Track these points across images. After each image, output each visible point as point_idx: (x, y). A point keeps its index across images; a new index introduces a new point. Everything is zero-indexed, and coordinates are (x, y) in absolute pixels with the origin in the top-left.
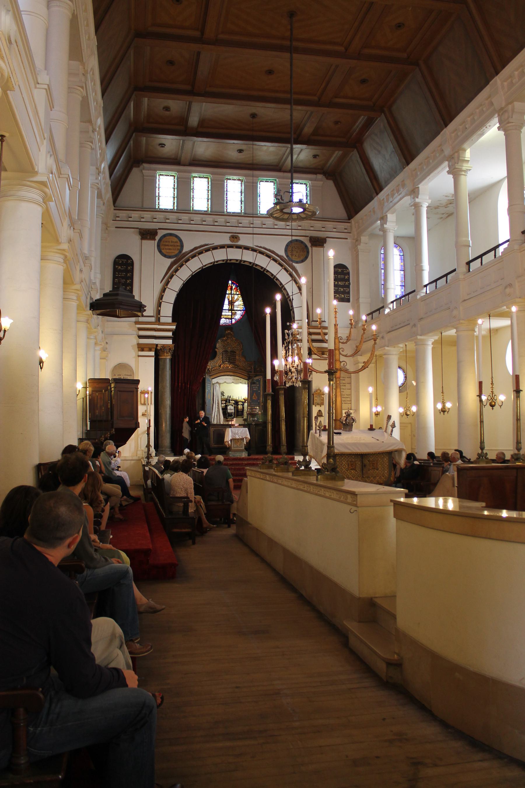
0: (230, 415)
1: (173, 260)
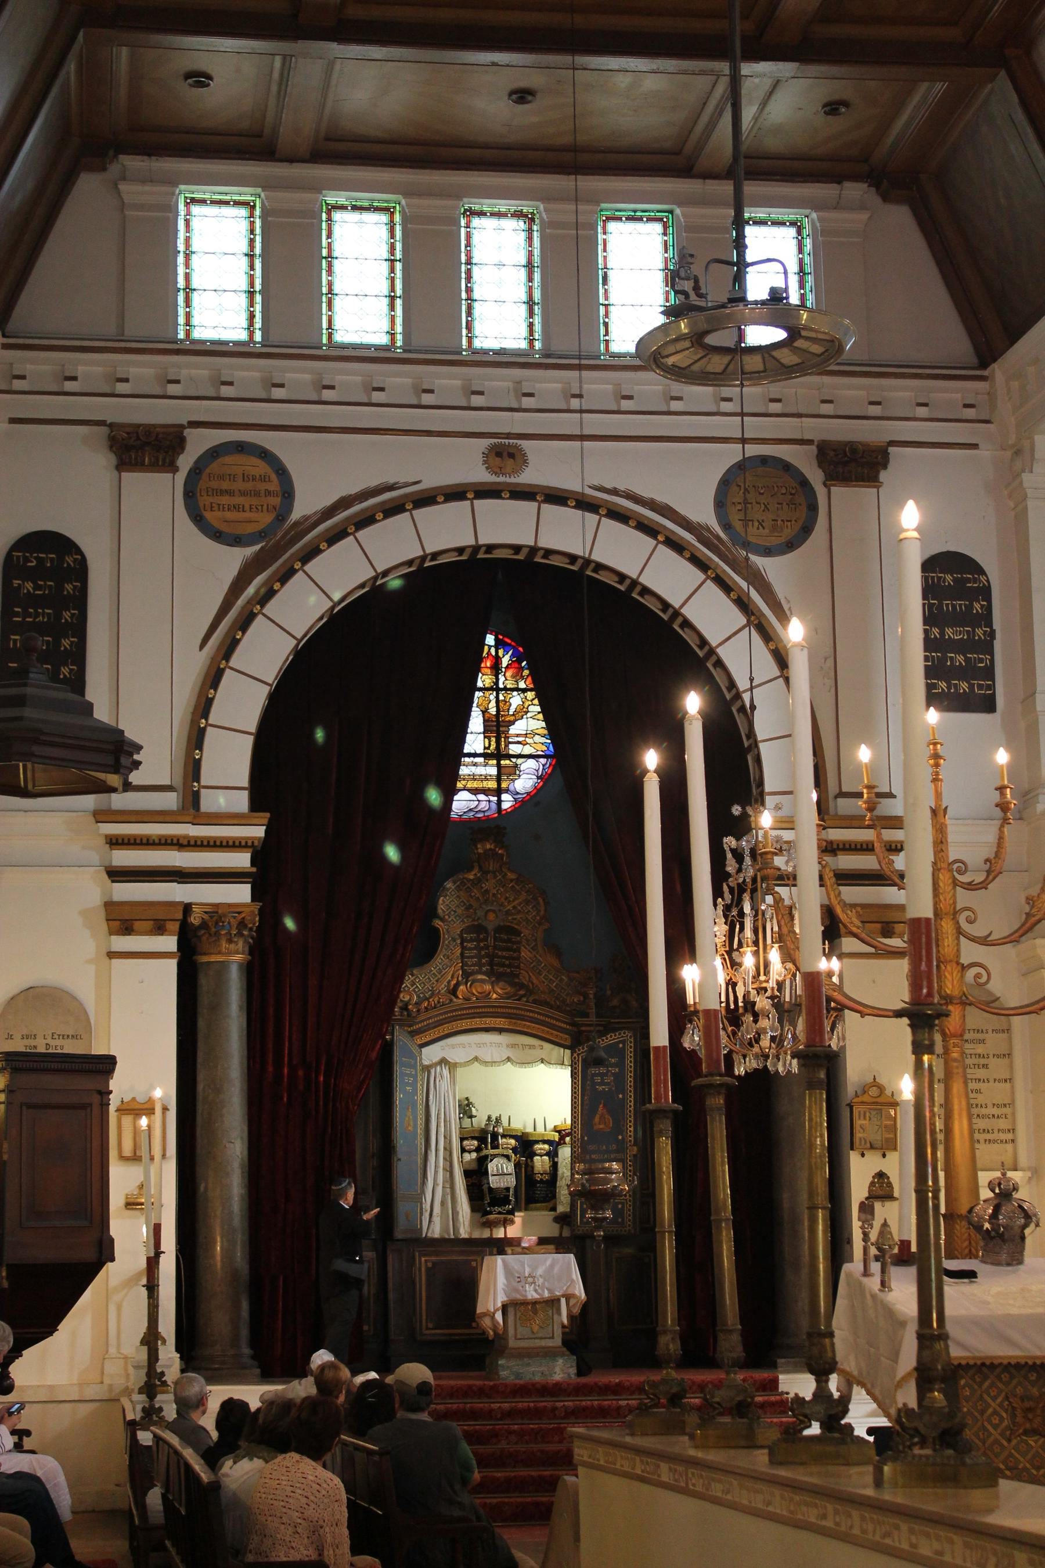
0: (499, 1198)
1: (250, 551)
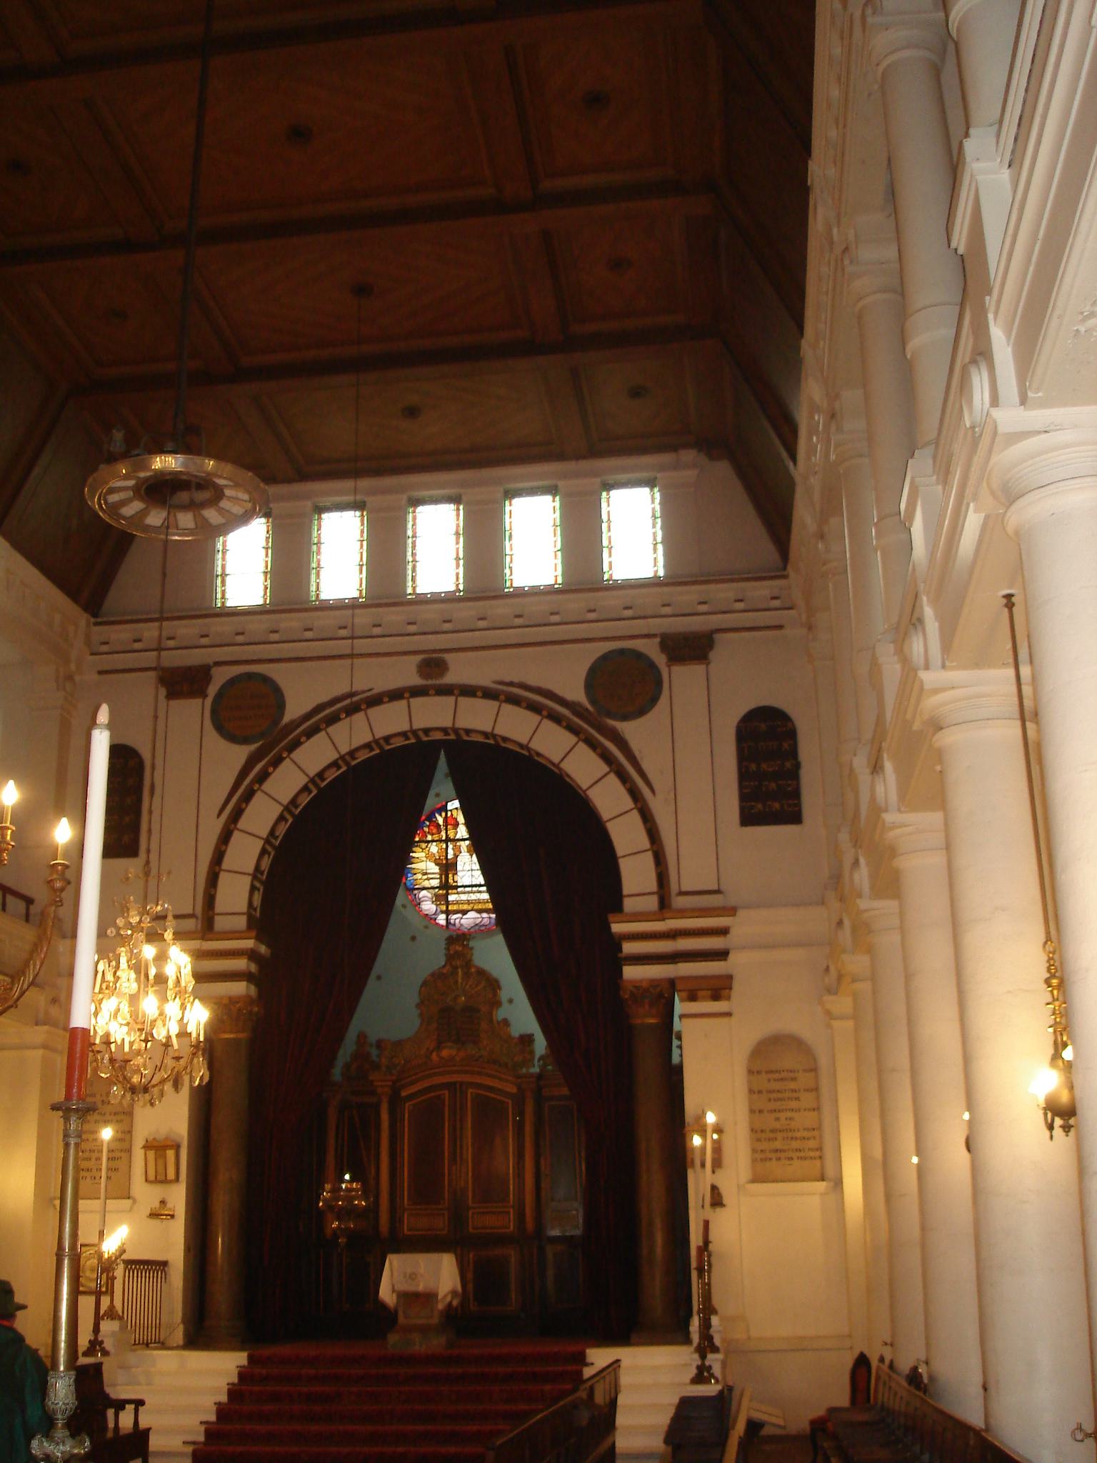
1: (253, 747)
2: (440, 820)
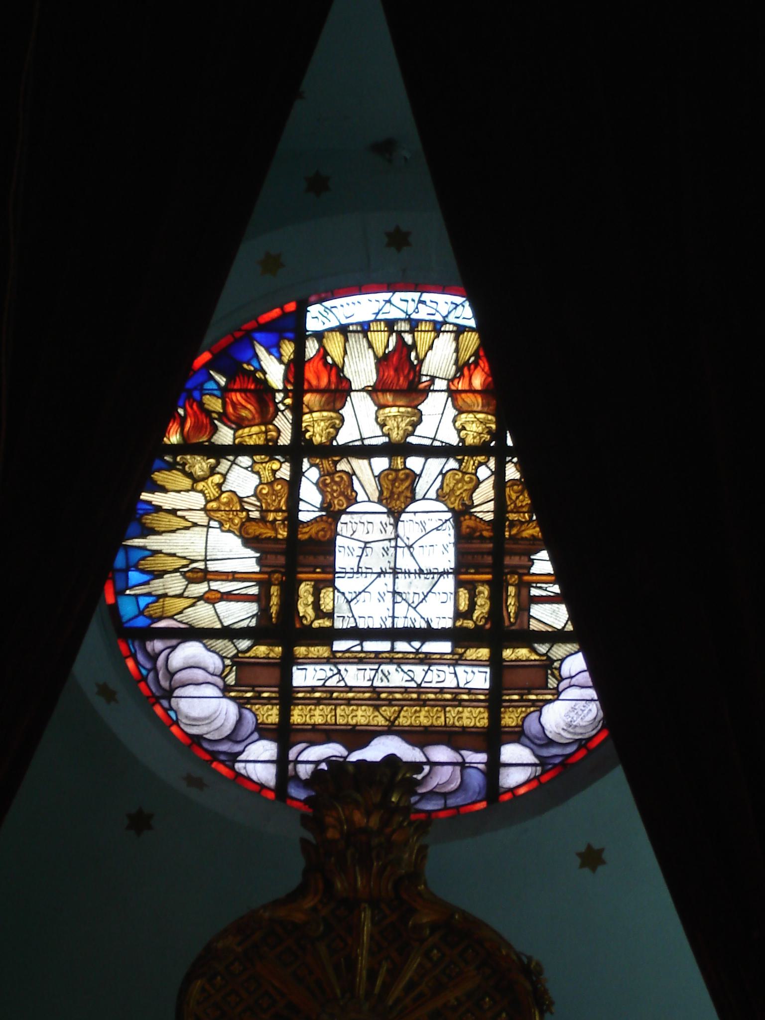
2: (274, 373)
